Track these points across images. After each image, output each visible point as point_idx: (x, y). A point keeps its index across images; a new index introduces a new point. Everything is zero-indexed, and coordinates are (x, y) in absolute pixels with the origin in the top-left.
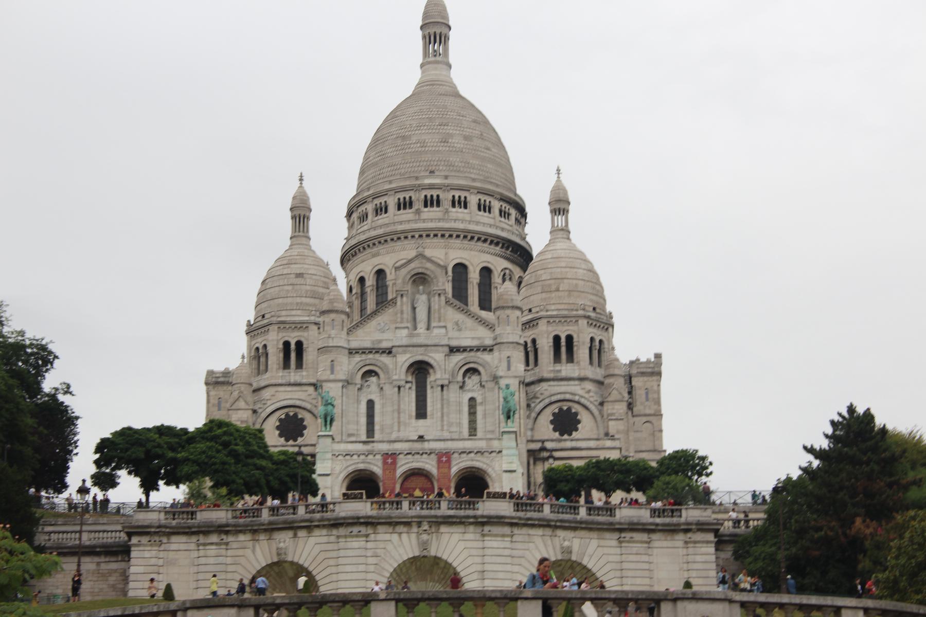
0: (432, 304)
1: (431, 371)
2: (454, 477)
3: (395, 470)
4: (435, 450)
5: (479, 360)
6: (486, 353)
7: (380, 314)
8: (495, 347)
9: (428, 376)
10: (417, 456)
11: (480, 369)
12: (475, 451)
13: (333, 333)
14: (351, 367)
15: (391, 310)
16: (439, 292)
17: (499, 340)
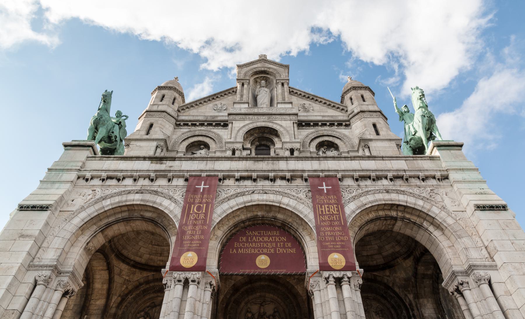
0: (275, 92)
1: (276, 140)
2: (351, 224)
3: (210, 207)
4: (303, 171)
5: (334, 134)
6: (340, 127)
7: (218, 99)
8: (351, 121)
9: (272, 147)
10: (261, 183)
11: (337, 141)
12: (390, 175)
13: (161, 103)
14: (174, 137)
15: (229, 98)
16: (282, 81)
17: (356, 111)
